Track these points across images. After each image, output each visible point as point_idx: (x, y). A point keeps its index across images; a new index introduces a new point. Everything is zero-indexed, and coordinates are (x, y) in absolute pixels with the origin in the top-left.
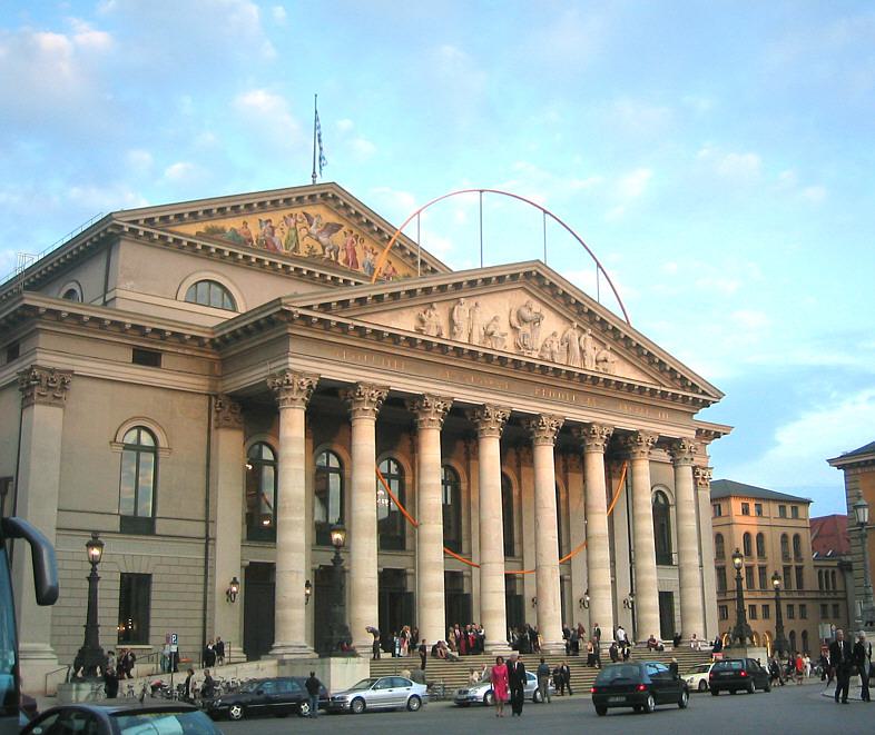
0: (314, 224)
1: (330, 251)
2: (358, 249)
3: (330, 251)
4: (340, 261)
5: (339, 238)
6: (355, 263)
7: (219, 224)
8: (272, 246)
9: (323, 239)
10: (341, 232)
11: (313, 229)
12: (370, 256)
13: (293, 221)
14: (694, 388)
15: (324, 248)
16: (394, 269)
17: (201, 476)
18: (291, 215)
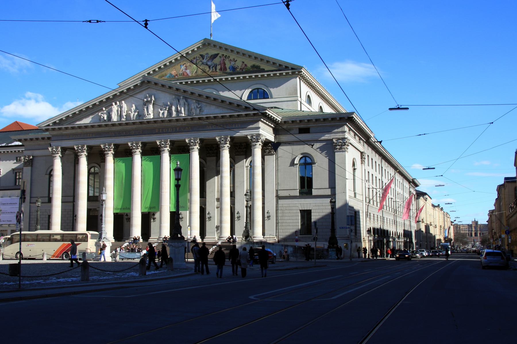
0: (205, 58)
1: (213, 67)
2: (227, 62)
3: (213, 67)
4: (218, 70)
5: (217, 60)
6: (225, 69)
7: (164, 73)
8: (185, 74)
9: (209, 63)
10: (218, 57)
11: (205, 61)
12: (233, 63)
13: (195, 60)
14: (247, 108)
15: (209, 67)
16: (246, 65)
17: (72, 182)
18: (194, 58)
